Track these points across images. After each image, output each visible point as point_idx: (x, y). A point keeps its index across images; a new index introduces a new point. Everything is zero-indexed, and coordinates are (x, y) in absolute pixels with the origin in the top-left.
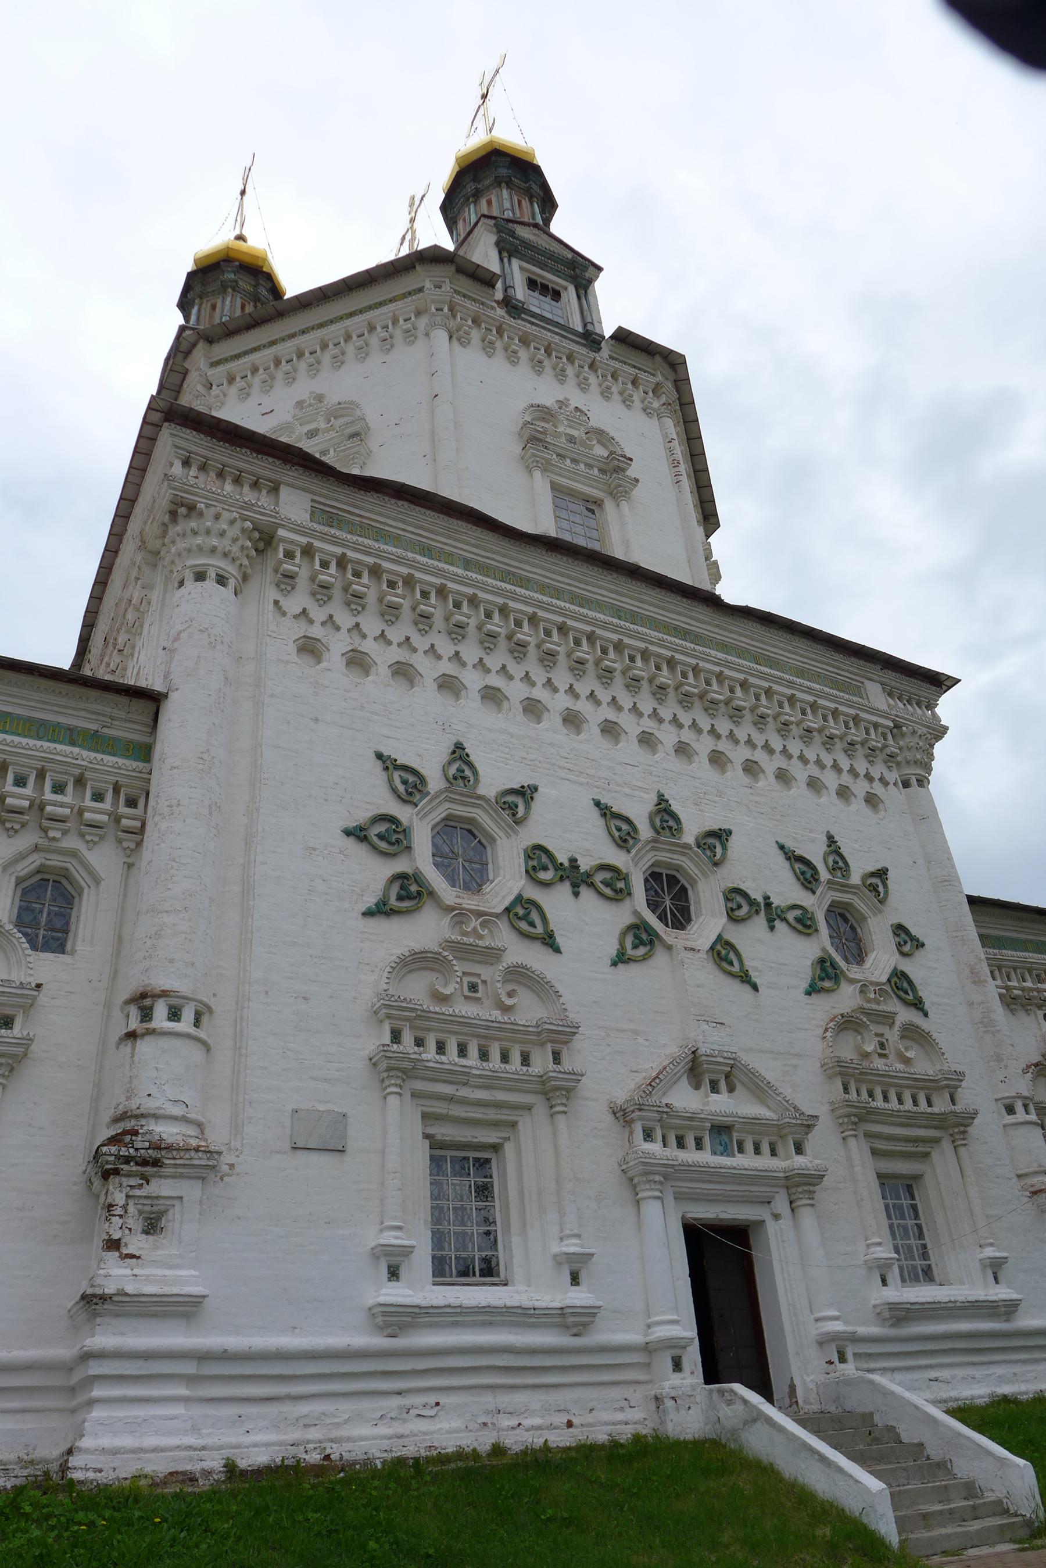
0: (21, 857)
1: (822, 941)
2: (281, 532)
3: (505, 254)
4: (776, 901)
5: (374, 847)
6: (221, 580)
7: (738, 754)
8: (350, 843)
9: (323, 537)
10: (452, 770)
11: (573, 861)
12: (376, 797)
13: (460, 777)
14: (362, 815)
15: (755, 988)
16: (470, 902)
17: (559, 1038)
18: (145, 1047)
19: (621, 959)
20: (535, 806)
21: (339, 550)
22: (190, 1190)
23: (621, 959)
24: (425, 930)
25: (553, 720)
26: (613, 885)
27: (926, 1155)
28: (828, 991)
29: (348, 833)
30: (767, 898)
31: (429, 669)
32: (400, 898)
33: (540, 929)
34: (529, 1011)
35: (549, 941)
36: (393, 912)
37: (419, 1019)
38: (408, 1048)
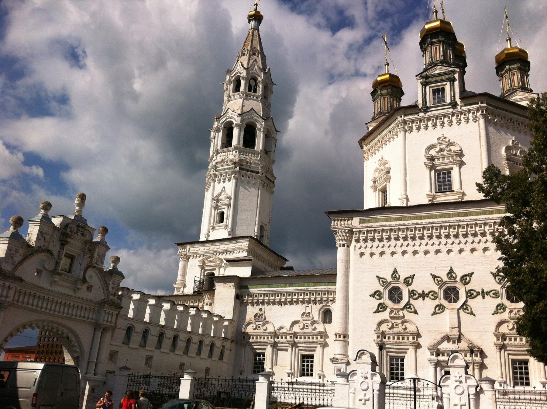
2: (354, 230)
4: (485, 291)
6: (344, 246)
11: (423, 291)
15: (474, 315)
16: (396, 306)
19: (435, 313)
23: (435, 313)
24: (385, 315)
26: (434, 295)
28: (501, 313)
29: (371, 296)
30: (483, 290)
32: (381, 308)
34: (411, 328)
35: (415, 312)
36: (379, 312)
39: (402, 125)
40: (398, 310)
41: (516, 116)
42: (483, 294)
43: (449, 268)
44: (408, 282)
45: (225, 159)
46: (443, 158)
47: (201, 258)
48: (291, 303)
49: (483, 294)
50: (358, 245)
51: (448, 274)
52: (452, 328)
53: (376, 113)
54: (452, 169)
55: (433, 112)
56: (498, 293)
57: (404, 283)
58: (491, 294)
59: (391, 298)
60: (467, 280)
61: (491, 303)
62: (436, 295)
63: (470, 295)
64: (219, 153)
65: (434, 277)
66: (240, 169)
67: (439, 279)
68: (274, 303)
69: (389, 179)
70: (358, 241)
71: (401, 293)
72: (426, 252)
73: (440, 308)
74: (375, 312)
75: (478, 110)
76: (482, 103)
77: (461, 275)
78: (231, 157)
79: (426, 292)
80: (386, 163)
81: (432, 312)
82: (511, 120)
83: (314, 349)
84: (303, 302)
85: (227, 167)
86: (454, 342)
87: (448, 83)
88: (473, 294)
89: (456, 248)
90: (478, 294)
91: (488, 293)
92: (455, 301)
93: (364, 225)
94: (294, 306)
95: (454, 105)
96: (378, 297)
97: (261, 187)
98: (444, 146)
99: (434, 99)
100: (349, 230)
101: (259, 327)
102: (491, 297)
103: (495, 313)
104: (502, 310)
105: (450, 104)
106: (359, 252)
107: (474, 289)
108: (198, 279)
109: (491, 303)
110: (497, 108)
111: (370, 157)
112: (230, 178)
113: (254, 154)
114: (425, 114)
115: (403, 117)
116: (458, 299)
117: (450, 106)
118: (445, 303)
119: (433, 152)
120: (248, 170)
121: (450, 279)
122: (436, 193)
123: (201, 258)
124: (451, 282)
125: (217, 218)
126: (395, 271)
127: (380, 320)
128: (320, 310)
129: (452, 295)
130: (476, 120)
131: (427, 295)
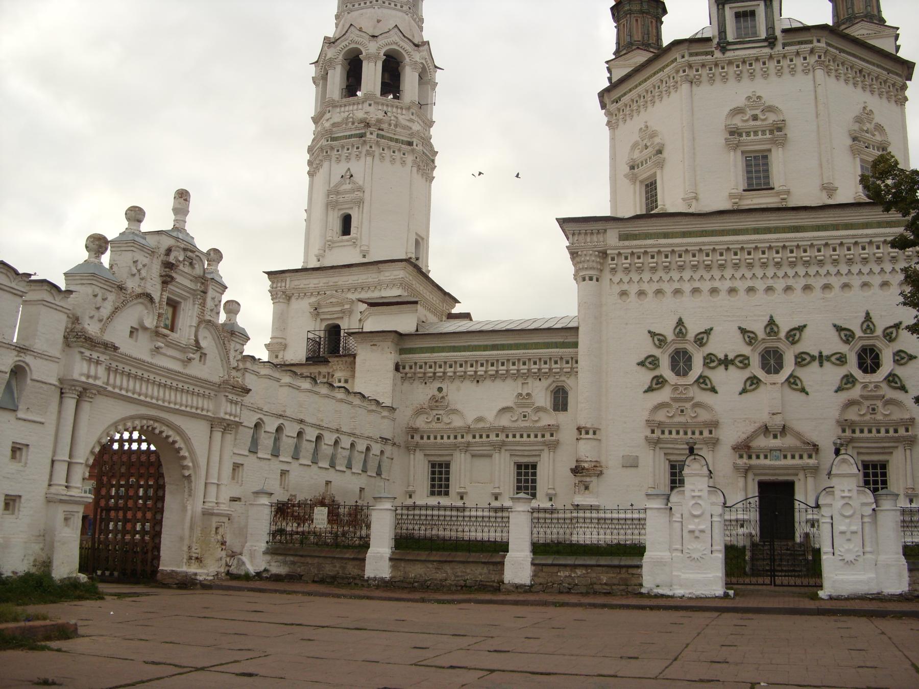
0: (550, 385)
1: (852, 367)
2: (608, 252)
3: (720, 7)
4: (824, 354)
5: (648, 368)
6: (591, 279)
7: (818, 283)
8: (639, 367)
9: (624, 248)
10: (677, 330)
11: (726, 356)
12: (648, 348)
13: (681, 332)
14: (642, 357)
15: (807, 394)
16: (681, 381)
17: (713, 425)
18: (581, 442)
19: (744, 391)
20: (711, 337)
21: (630, 251)
22: (594, 479)
23: (744, 391)
24: (664, 395)
25: (723, 294)
26: (743, 362)
27: (892, 453)
28: (847, 389)
29: (638, 364)
30: (821, 353)
31: (668, 288)
32: (656, 384)
33: (709, 386)
34: (704, 416)
35: (713, 390)
37: (660, 424)
38: (657, 433)
39: (684, 71)
40: (686, 387)
41: (871, 67)
42: (821, 359)
43: (768, 318)
44: (701, 340)
45: (347, 118)
46: (756, 133)
47: (313, 300)
48: (496, 376)
49: (821, 359)
50: (616, 279)
51: (766, 327)
52: (773, 414)
53: (622, 44)
54: (770, 150)
55: (738, 53)
56: (845, 357)
57: (695, 342)
58: (833, 359)
59: (674, 367)
60: (797, 338)
61: (833, 374)
62: (746, 362)
63: (801, 360)
64: (336, 106)
65: (743, 331)
66: (378, 136)
67: (752, 335)
68: (464, 377)
69: (661, 165)
70: (613, 270)
71: (690, 359)
72: (732, 291)
73: (754, 382)
74: (645, 392)
75: (812, 51)
76: (819, 41)
77: (787, 329)
78: (360, 115)
79: (731, 357)
80: (653, 135)
81: (740, 389)
82: (861, 71)
83: (537, 453)
84: (517, 376)
85: (353, 133)
86: (775, 437)
87: (762, 4)
88: (804, 359)
89: (780, 285)
90: (813, 358)
91: (828, 358)
92: (777, 372)
93: (627, 243)
94: (498, 384)
95: (771, 41)
96: (651, 366)
97: (415, 169)
98: (757, 112)
99: (738, 28)
100: (599, 252)
101: (438, 419)
102: (833, 363)
103: (839, 389)
104: (849, 386)
105: (765, 40)
106: (617, 289)
107: (807, 351)
108: (311, 336)
109: (833, 374)
110: (841, 51)
111: (621, 123)
112: (360, 152)
113: (402, 108)
114: (724, 53)
115: (687, 58)
116: (781, 367)
117: (766, 44)
118: (761, 374)
119: (737, 121)
120: (391, 139)
121: (769, 334)
122: (744, 190)
123: (313, 300)
124: (772, 341)
125: (337, 225)
126: (680, 322)
127: (656, 403)
128: (547, 389)
129: (772, 362)
130: (806, 71)
131: (732, 362)
